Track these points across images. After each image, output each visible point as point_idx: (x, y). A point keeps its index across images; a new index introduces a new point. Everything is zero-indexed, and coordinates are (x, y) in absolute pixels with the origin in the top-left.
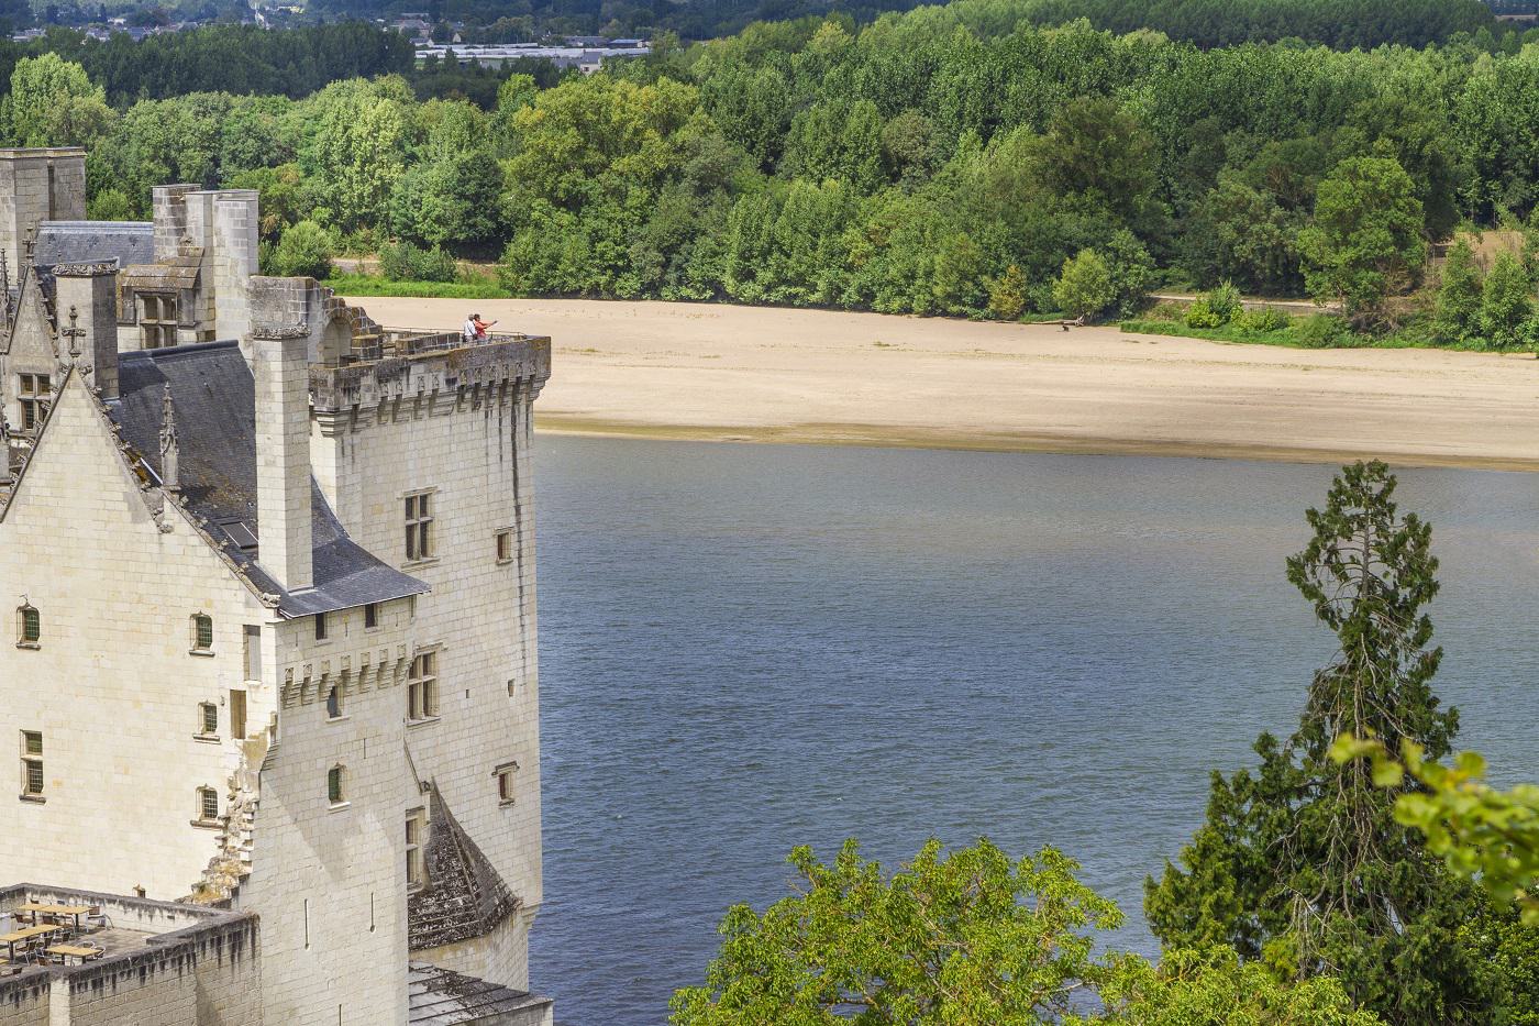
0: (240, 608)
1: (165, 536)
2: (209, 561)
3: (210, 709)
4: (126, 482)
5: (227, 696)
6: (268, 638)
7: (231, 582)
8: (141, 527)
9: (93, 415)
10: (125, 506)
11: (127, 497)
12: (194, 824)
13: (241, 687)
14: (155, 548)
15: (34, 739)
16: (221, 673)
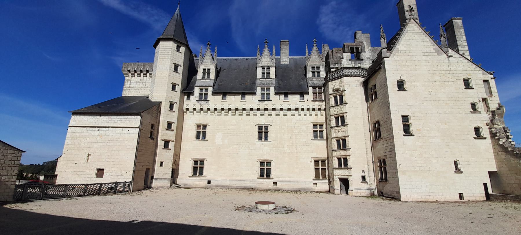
0: (481, 76)
1: (451, 58)
2: (468, 64)
4: (434, 45)
5: (481, 100)
6: (492, 83)
7: (476, 69)
8: (440, 56)
9: (419, 30)
10: (434, 51)
11: (434, 49)
12: (475, 138)
13: (485, 97)
14: (448, 61)
15: (405, 118)
16: (478, 92)
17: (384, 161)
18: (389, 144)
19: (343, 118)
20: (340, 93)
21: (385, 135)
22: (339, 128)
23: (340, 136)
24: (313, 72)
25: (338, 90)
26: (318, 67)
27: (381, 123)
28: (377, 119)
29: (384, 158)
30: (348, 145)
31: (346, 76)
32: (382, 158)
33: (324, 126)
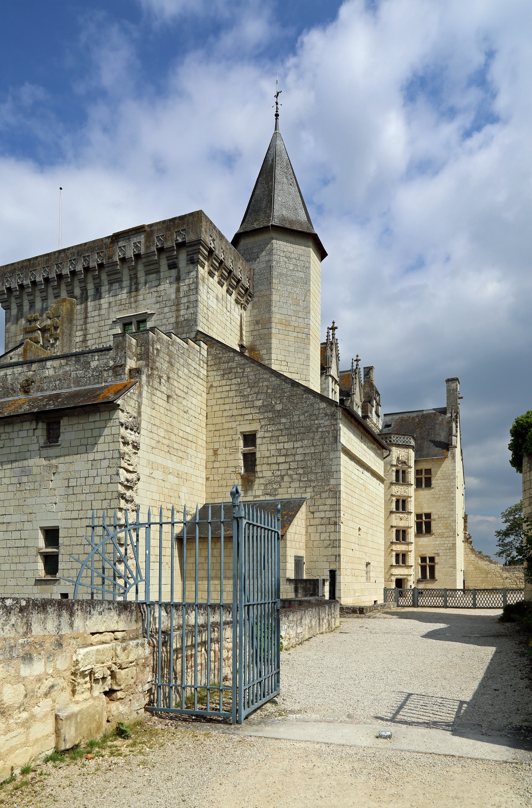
21: (439, 531)
28: (427, 511)
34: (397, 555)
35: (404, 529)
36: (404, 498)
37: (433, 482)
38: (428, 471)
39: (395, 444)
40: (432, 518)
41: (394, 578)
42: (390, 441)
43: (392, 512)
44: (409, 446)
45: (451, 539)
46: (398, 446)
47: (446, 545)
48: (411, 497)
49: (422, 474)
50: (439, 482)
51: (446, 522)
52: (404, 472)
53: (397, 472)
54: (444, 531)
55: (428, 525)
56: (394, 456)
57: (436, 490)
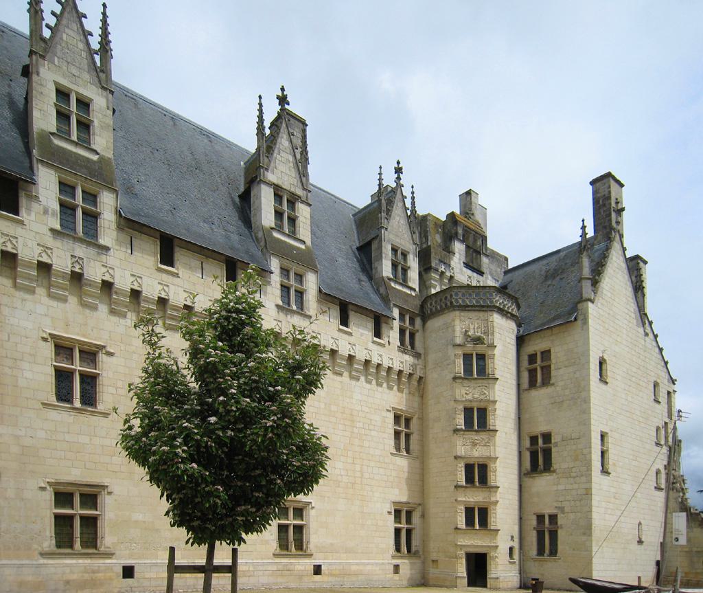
3: (658, 429)
17: (553, 518)
18: (576, 486)
19: (483, 413)
20: (480, 349)
22: (475, 437)
23: (476, 454)
24: (395, 266)
25: (478, 340)
26: (405, 255)
27: (555, 439)
28: (543, 428)
29: (553, 511)
30: (492, 479)
31: (501, 311)
32: (547, 511)
33: (414, 423)
34: (469, 512)
35: (481, 461)
36: (482, 405)
37: (553, 373)
38: (546, 354)
39: (460, 306)
40: (553, 441)
41: (462, 553)
42: (451, 303)
43: (456, 431)
44: (488, 307)
45: (583, 479)
46: (465, 308)
47: (574, 492)
48: (495, 402)
49: (536, 363)
50: (561, 371)
51: (574, 447)
52: (482, 357)
53: (467, 358)
54: (571, 465)
55: (548, 453)
56: (458, 328)
57: (558, 389)
